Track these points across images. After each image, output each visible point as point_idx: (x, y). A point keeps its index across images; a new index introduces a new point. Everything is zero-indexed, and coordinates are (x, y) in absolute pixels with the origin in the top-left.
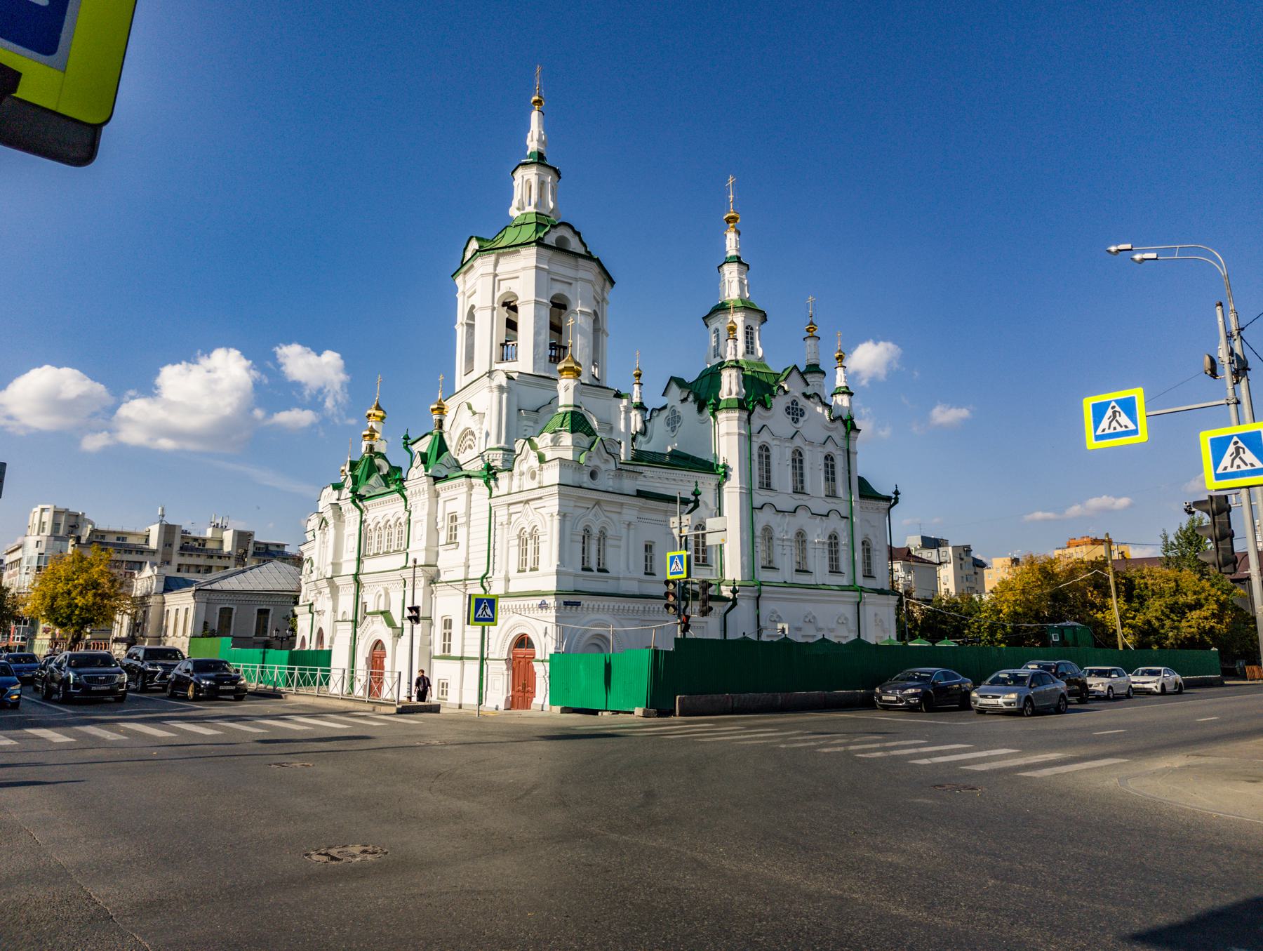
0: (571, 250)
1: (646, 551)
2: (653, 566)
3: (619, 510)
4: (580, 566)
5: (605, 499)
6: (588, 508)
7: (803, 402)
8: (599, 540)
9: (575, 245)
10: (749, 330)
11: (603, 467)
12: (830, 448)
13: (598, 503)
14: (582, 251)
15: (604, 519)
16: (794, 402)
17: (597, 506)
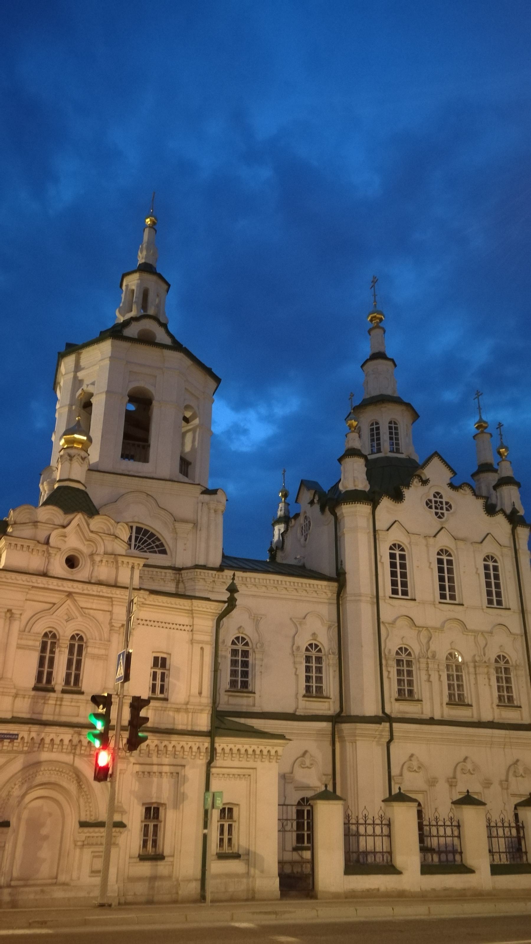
0: (156, 341)
1: (155, 664)
2: (166, 687)
3: (106, 608)
4: (32, 682)
5: (119, 596)
6: (54, 604)
7: (448, 494)
8: (71, 647)
9: (161, 336)
10: (393, 425)
11: (85, 550)
12: (489, 548)
13: (70, 594)
14: (168, 341)
15: (80, 619)
16: (437, 494)
17: (69, 602)
